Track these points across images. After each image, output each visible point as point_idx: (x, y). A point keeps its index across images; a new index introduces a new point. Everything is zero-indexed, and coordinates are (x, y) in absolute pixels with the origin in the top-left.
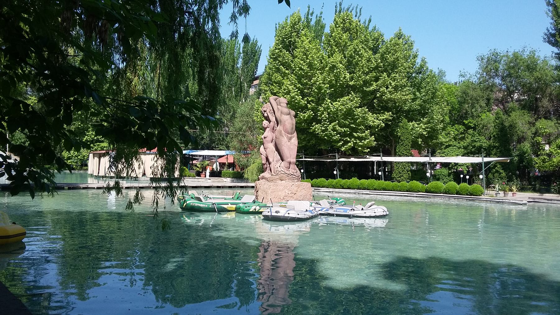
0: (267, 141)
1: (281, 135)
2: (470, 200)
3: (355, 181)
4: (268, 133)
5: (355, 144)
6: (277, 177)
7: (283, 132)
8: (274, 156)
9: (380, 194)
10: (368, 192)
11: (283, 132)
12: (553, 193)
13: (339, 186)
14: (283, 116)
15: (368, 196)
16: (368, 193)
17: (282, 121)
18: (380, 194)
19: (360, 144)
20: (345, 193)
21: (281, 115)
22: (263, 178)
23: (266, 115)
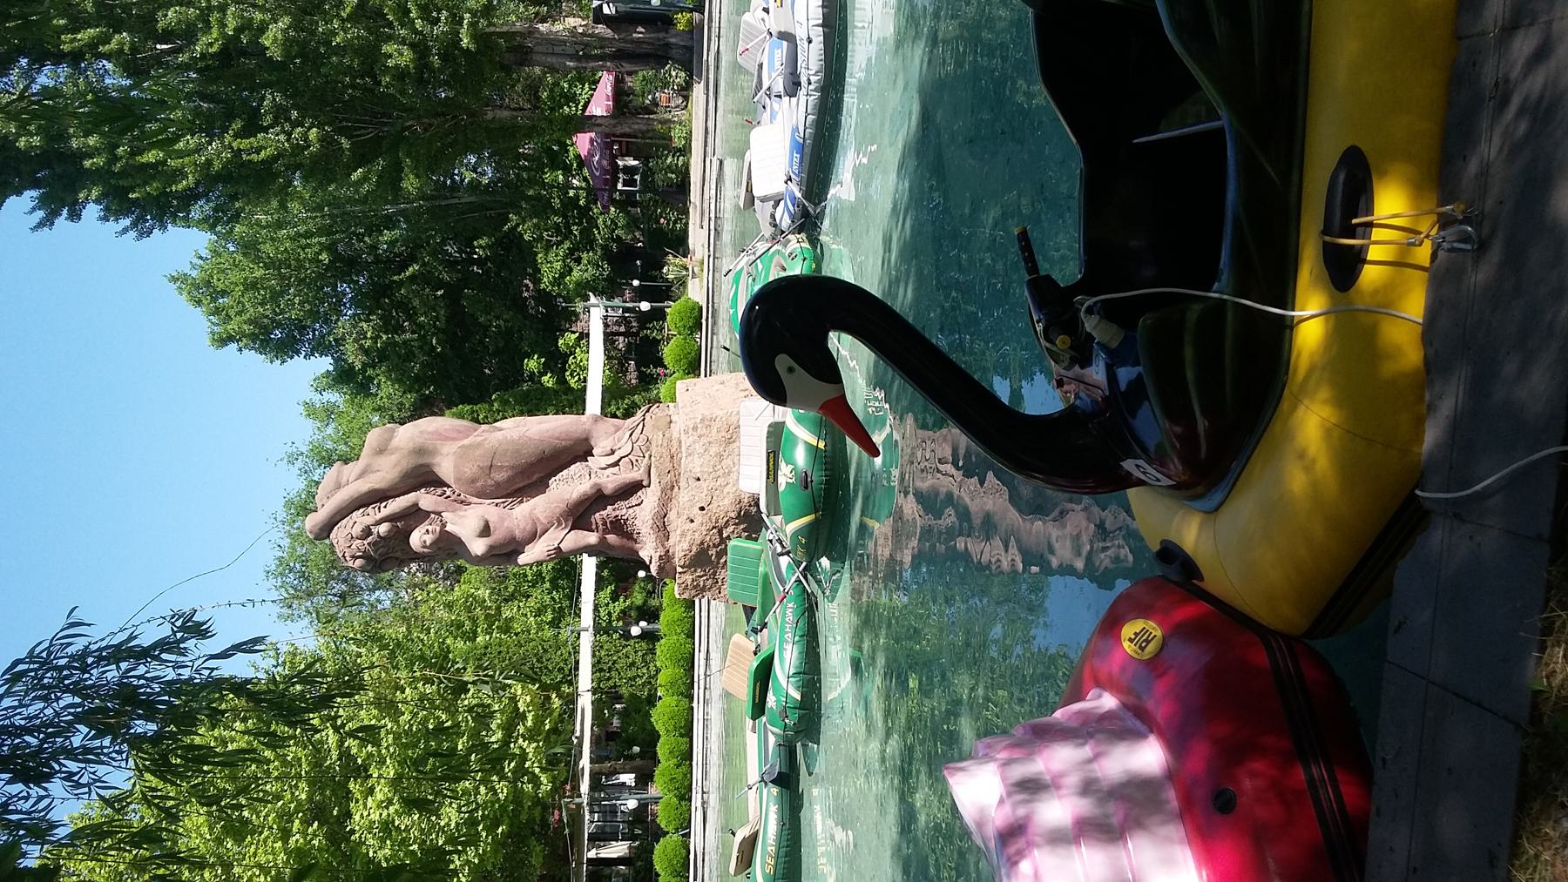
0: (502, 520)
1: (479, 445)
2: (714, 323)
3: (660, 717)
4: (466, 523)
5: (531, 736)
6: (657, 438)
7: (466, 442)
8: (570, 485)
9: (704, 614)
10: (700, 659)
11: (466, 442)
12: (687, 224)
13: (684, 769)
14: (395, 442)
15: (712, 655)
16: (703, 655)
17: (419, 440)
18: (704, 614)
19: (529, 723)
20: (705, 738)
21: (397, 449)
22: (662, 529)
23: (383, 528)
